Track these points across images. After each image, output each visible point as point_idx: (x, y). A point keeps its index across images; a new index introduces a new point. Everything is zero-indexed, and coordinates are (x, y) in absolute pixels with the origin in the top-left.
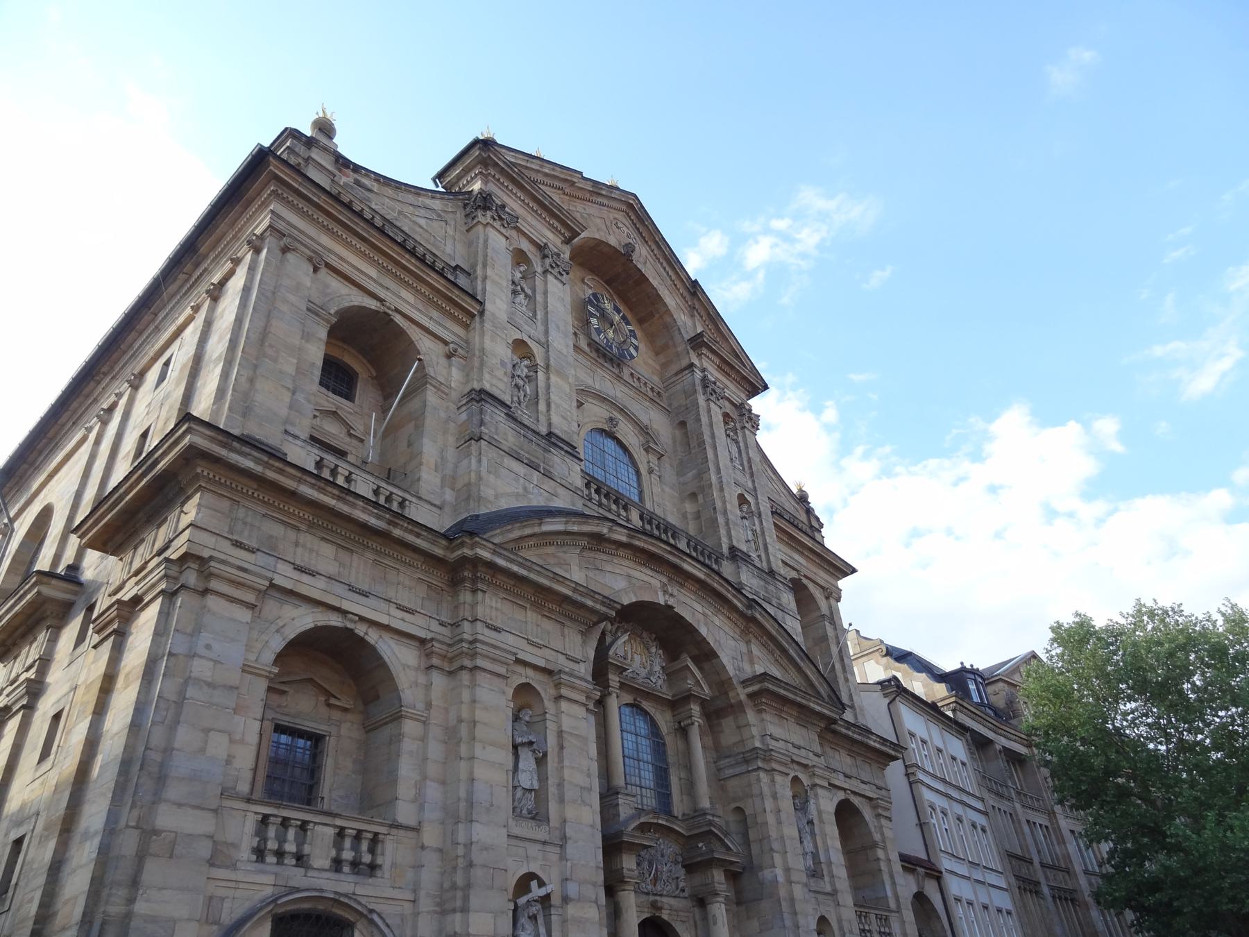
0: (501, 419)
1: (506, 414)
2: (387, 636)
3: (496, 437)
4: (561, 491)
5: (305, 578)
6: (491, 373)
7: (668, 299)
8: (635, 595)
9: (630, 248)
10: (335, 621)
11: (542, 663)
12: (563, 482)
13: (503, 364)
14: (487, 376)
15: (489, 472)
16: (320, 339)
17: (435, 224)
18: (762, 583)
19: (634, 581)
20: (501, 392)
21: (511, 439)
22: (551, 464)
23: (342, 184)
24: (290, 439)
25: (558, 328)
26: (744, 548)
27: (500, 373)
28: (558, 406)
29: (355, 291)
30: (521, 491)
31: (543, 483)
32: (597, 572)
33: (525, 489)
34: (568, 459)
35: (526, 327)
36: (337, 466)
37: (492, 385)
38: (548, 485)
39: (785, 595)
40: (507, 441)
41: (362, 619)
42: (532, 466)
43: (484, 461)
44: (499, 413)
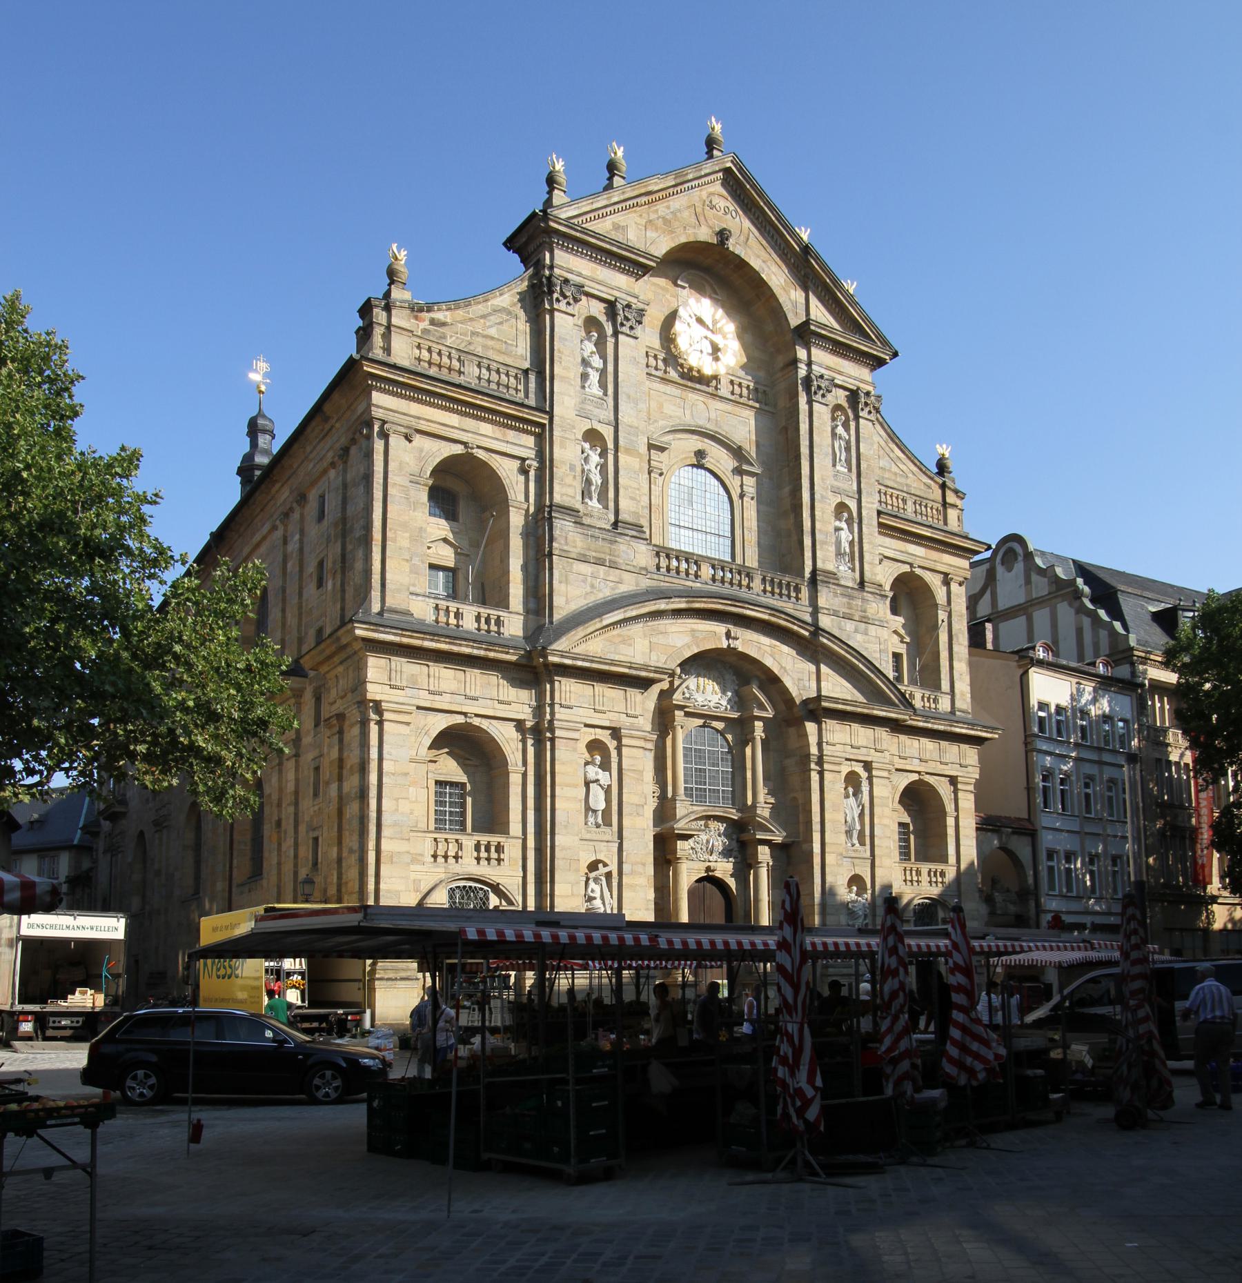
0: (571, 529)
1: (575, 522)
2: (492, 721)
3: (565, 548)
4: (626, 576)
5: (437, 698)
6: (562, 484)
7: (773, 277)
8: (698, 646)
9: (723, 235)
10: (460, 719)
11: (607, 724)
12: (628, 568)
13: (572, 468)
14: (556, 487)
15: (560, 582)
16: (423, 504)
17: (505, 327)
18: (845, 600)
19: (697, 634)
20: (570, 499)
21: (579, 544)
22: (616, 554)
23: (419, 334)
24: (414, 597)
25: (629, 397)
26: (830, 567)
27: (569, 480)
28: (626, 488)
29: (444, 443)
30: (588, 589)
31: (609, 575)
32: (660, 636)
33: (592, 586)
34: (634, 543)
35: (596, 411)
36: (448, 607)
37: (562, 495)
38: (614, 574)
39: (874, 604)
40: (575, 547)
41: (477, 715)
42: (599, 562)
43: (556, 573)
44: (568, 523)
